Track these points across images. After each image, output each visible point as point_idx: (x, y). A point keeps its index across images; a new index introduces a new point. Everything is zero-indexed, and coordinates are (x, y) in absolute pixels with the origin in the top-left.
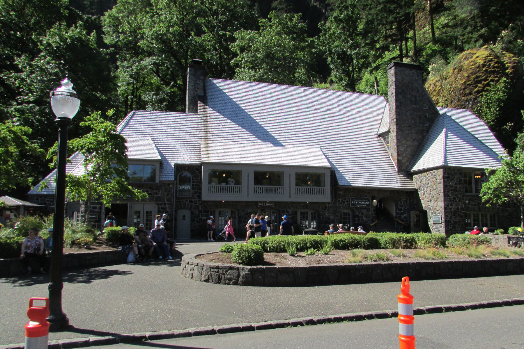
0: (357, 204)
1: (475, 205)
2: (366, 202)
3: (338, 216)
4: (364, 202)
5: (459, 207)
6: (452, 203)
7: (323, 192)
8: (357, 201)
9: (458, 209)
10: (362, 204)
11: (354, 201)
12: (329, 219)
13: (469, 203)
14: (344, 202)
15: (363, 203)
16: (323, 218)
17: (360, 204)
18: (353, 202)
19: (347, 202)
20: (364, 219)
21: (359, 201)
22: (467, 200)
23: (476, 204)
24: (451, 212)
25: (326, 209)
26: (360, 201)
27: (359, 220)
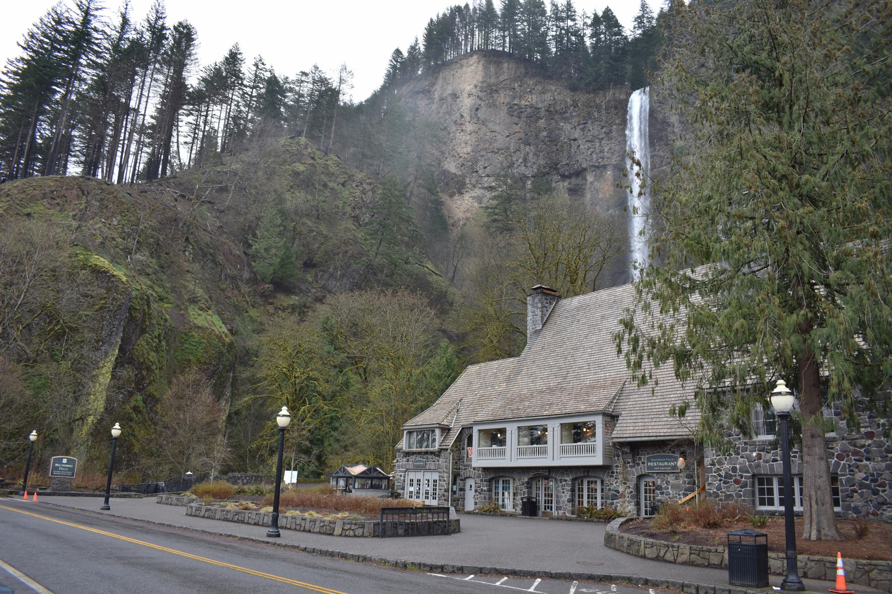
0: (657, 466)
1: (775, 460)
2: (670, 462)
3: (629, 487)
4: (668, 462)
5: (738, 466)
6: (719, 459)
7: (592, 450)
8: (656, 462)
9: (734, 469)
10: (665, 466)
11: (651, 462)
12: (618, 491)
13: (759, 457)
14: (638, 464)
15: (666, 464)
16: (610, 490)
17: (662, 466)
18: (649, 464)
19: (643, 463)
20: (671, 492)
21: (659, 462)
22: (752, 451)
23: (779, 458)
24: (720, 475)
25: (612, 476)
26: (661, 462)
27: (662, 493)
